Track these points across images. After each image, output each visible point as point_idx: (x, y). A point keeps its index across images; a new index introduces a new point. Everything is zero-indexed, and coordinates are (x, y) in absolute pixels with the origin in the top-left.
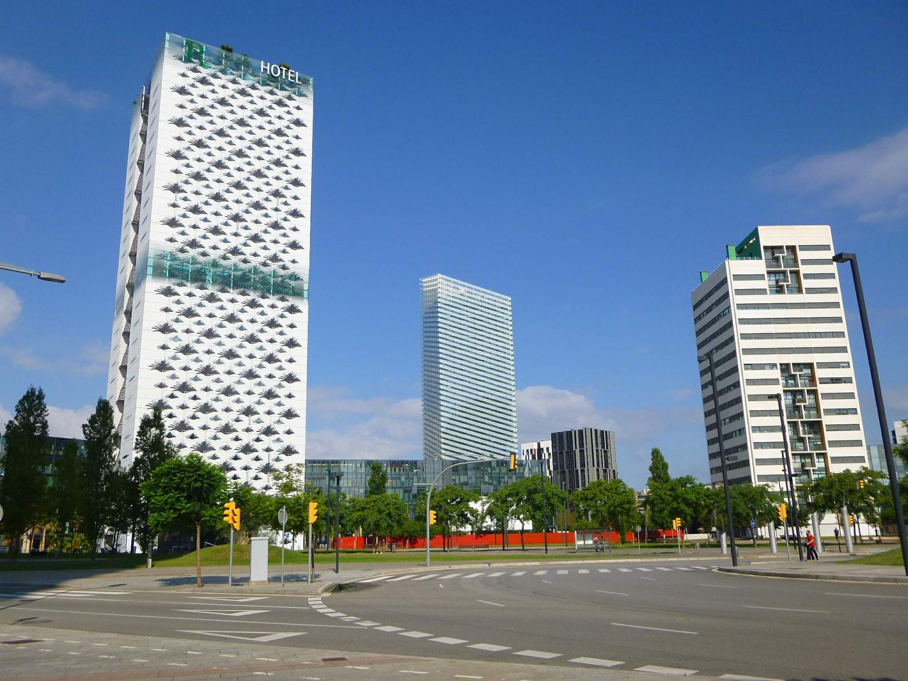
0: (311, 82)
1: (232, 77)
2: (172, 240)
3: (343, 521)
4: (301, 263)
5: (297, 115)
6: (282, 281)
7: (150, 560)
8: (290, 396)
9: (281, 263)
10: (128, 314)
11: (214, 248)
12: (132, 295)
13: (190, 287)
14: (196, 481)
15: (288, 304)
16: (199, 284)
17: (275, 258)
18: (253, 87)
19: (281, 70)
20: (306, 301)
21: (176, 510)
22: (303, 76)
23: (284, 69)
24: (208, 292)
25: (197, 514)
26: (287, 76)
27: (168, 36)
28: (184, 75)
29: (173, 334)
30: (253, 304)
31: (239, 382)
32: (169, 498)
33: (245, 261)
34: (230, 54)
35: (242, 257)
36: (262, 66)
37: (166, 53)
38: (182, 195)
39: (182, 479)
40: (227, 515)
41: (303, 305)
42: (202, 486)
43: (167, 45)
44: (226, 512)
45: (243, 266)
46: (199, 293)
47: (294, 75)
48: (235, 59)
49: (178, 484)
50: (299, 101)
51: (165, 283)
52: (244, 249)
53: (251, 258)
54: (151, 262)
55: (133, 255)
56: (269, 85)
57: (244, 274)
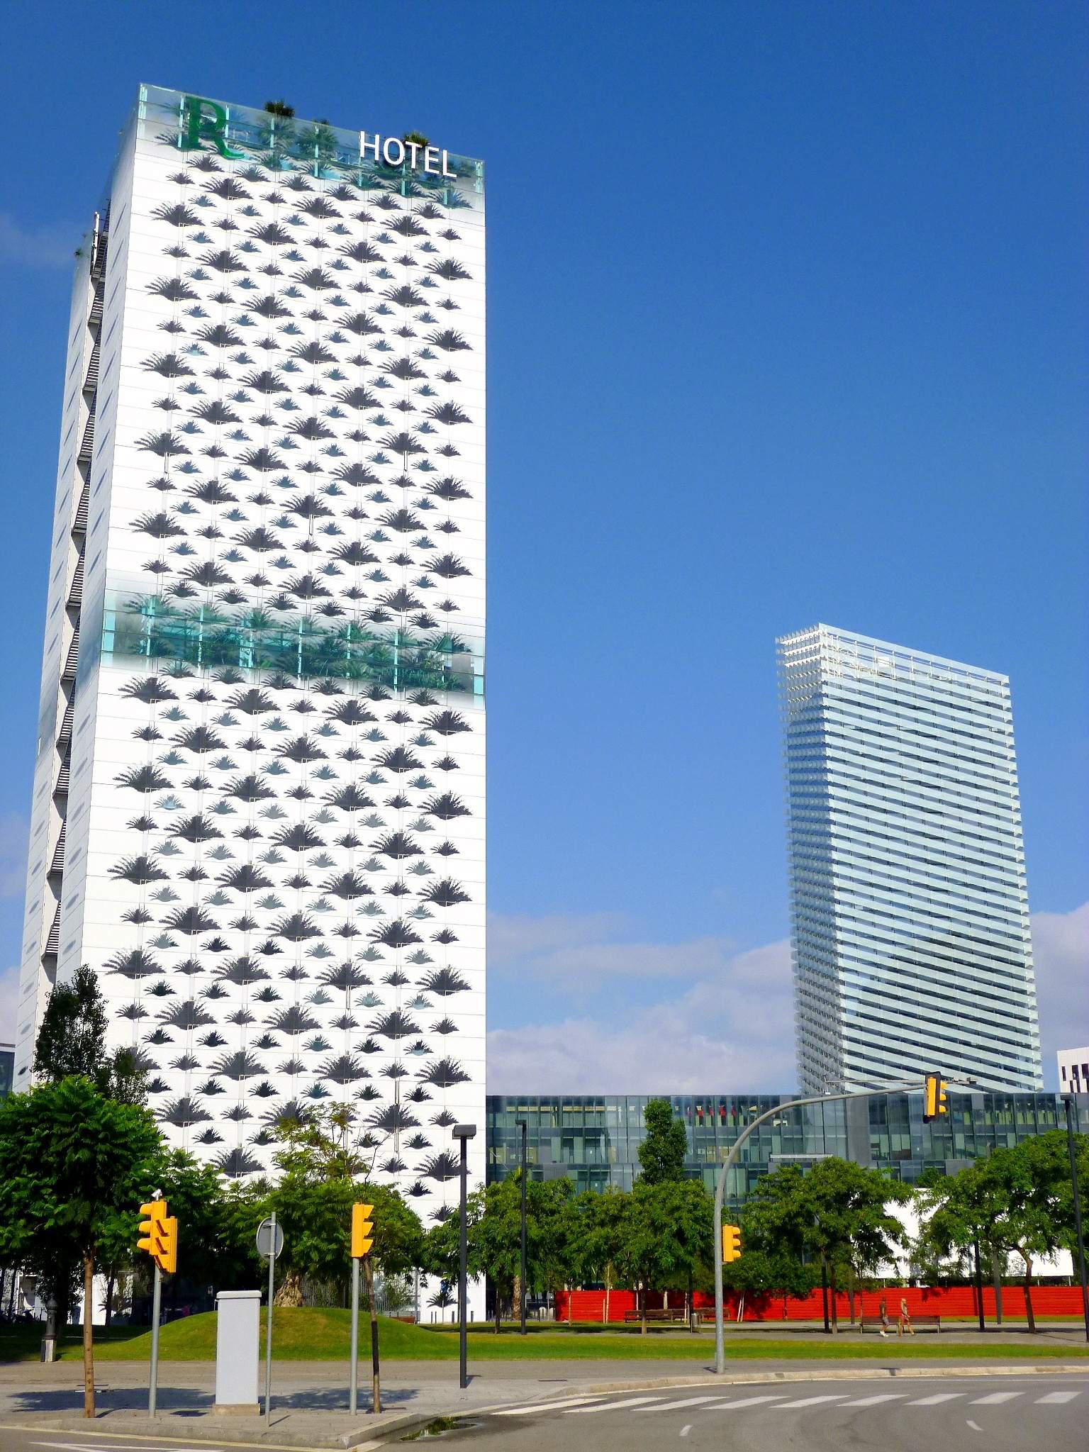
0: (479, 172)
1: (292, 175)
2: (157, 567)
3: (566, 1252)
4: (465, 610)
5: (447, 252)
6: (422, 656)
7: (50, 1344)
8: (445, 938)
9: (418, 612)
10: (65, 746)
11: (257, 582)
12: (71, 703)
13: (202, 679)
14: (77, 1145)
16: (222, 670)
17: (402, 601)
18: (342, 195)
19: (408, 148)
20: (479, 703)
21: (31, 1219)
22: (459, 158)
23: (414, 146)
24: (244, 688)
25: (85, 1228)
26: (420, 163)
27: (144, 93)
28: (181, 179)
29: (164, 793)
30: (351, 714)
31: (321, 905)
32: (17, 1188)
33: (331, 611)
34: (286, 122)
35: (324, 600)
36: (363, 144)
37: (141, 130)
38: (181, 459)
39: (46, 1141)
40: (147, 1235)
41: (473, 712)
42: (93, 1160)
43: (142, 113)
44: (143, 1226)
45: (325, 622)
46: (223, 691)
47: (438, 158)
48: (297, 132)
49: (37, 1153)
50: (451, 218)
51: (143, 671)
52: (327, 582)
53: (346, 603)
54: (110, 623)
55: (73, 608)
56: (378, 186)
57: (328, 641)
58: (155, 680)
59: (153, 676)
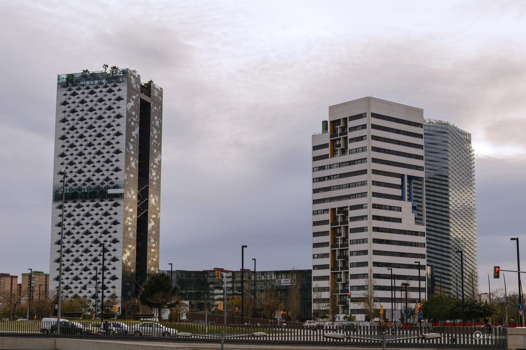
9: (111, 181)
15: (114, 202)
17: (107, 179)
35: (92, 182)
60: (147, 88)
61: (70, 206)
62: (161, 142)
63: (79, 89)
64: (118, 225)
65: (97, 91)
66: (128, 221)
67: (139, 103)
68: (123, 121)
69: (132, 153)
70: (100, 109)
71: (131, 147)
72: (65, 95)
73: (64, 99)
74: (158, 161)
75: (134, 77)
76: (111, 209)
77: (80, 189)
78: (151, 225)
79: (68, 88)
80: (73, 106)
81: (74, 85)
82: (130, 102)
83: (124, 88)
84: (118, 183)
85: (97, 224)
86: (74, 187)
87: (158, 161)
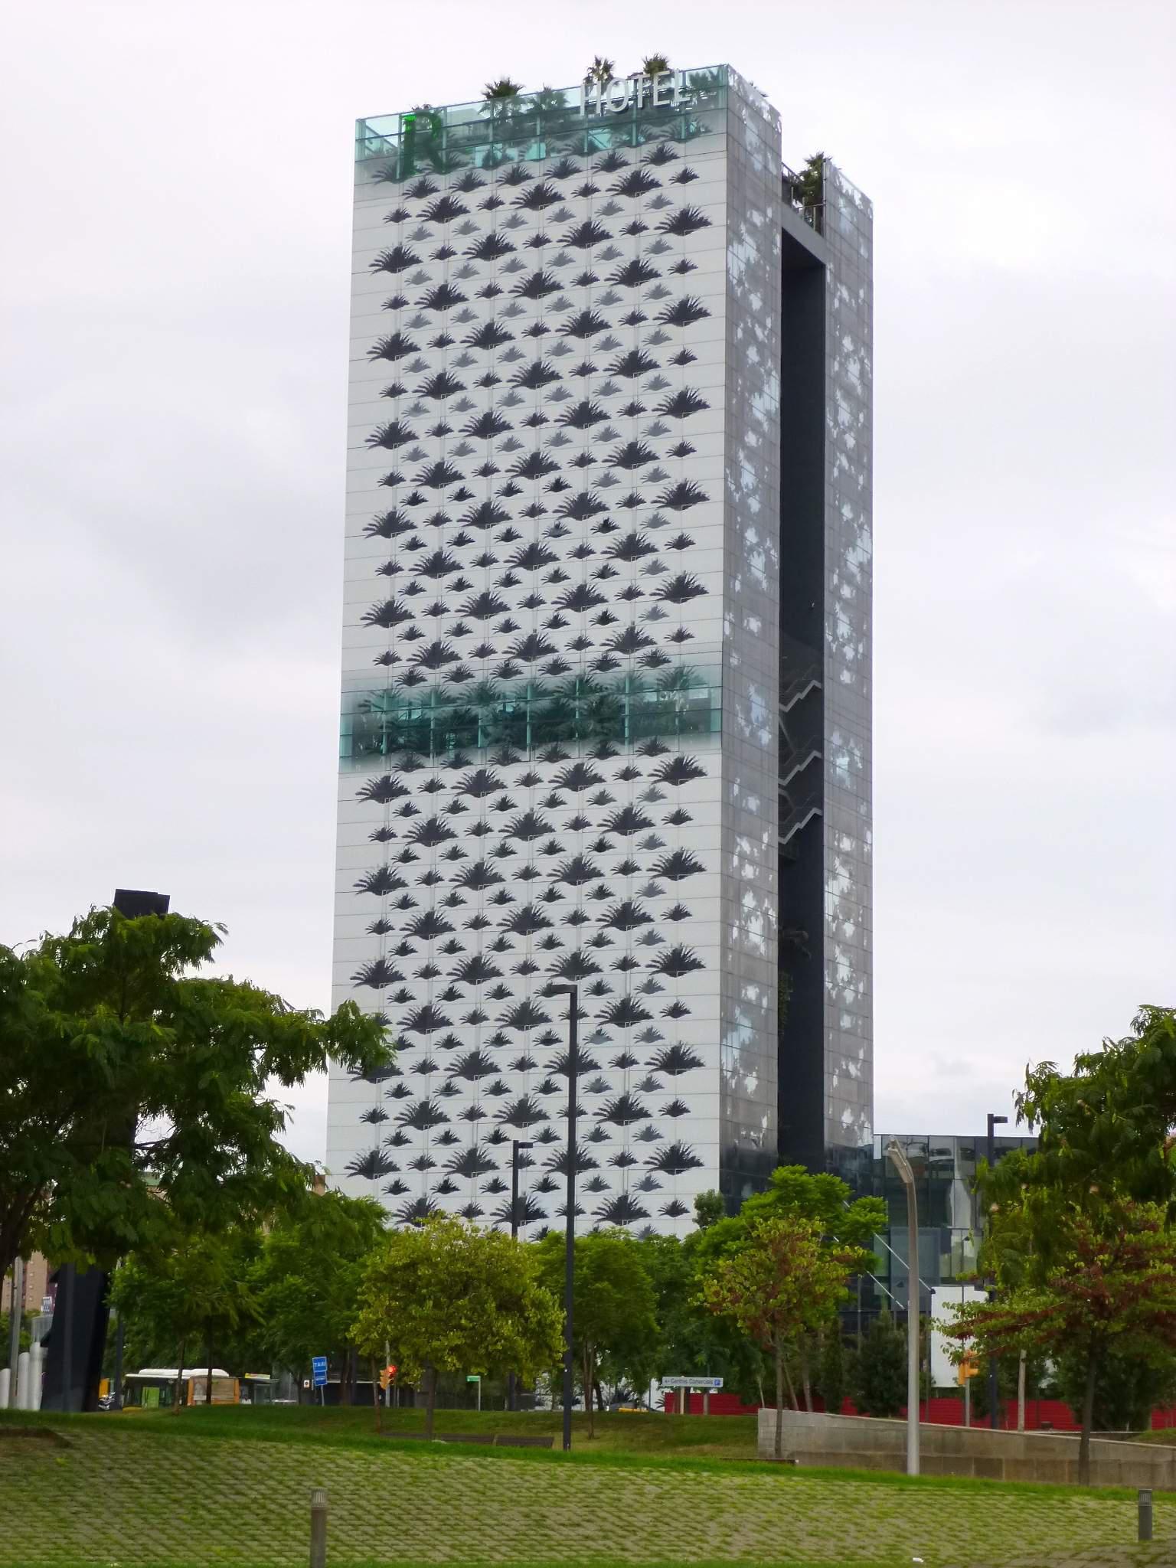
9: (648, 650)
15: (668, 759)
17: (631, 641)
35: (548, 659)
50: (687, 155)
57: (557, 701)
58: (387, 778)
59: (386, 774)
60: (812, 189)
61: (433, 785)
62: (868, 469)
63: (469, 185)
64: (696, 876)
65: (566, 187)
66: (743, 857)
67: (777, 251)
68: (706, 338)
69: (755, 505)
70: (585, 280)
71: (748, 479)
72: (399, 216)
73: (392, 237)
74: (861, 565)
75: (757, 113)
76: (653, 796)
77: (485, 695)
78: (835, 889)
79: (414, 181)
80: (439, 274)
81: (444, 167)
82: (741, 241)
83: (708, 161)
84: (689, 660)
85: (578, 872)
86: (455, 689)
87: (861, 565)
